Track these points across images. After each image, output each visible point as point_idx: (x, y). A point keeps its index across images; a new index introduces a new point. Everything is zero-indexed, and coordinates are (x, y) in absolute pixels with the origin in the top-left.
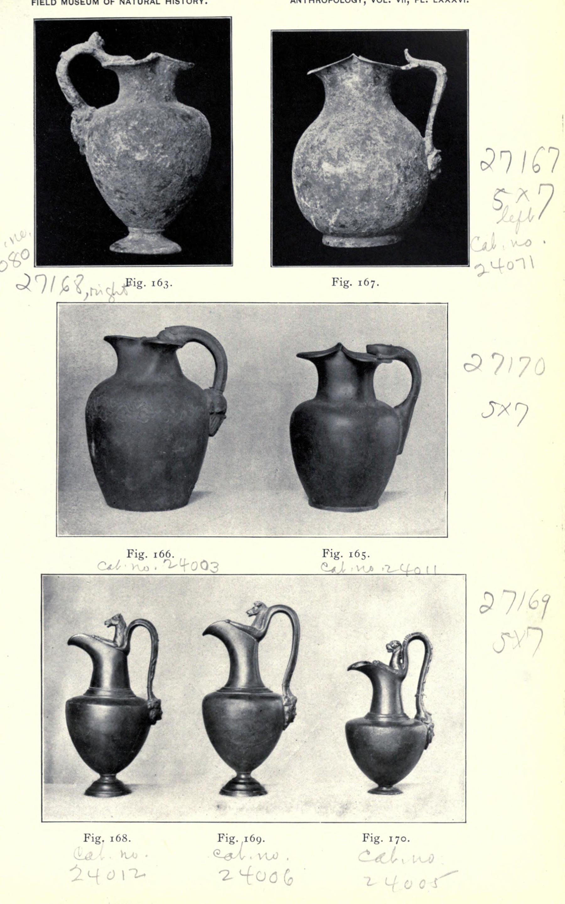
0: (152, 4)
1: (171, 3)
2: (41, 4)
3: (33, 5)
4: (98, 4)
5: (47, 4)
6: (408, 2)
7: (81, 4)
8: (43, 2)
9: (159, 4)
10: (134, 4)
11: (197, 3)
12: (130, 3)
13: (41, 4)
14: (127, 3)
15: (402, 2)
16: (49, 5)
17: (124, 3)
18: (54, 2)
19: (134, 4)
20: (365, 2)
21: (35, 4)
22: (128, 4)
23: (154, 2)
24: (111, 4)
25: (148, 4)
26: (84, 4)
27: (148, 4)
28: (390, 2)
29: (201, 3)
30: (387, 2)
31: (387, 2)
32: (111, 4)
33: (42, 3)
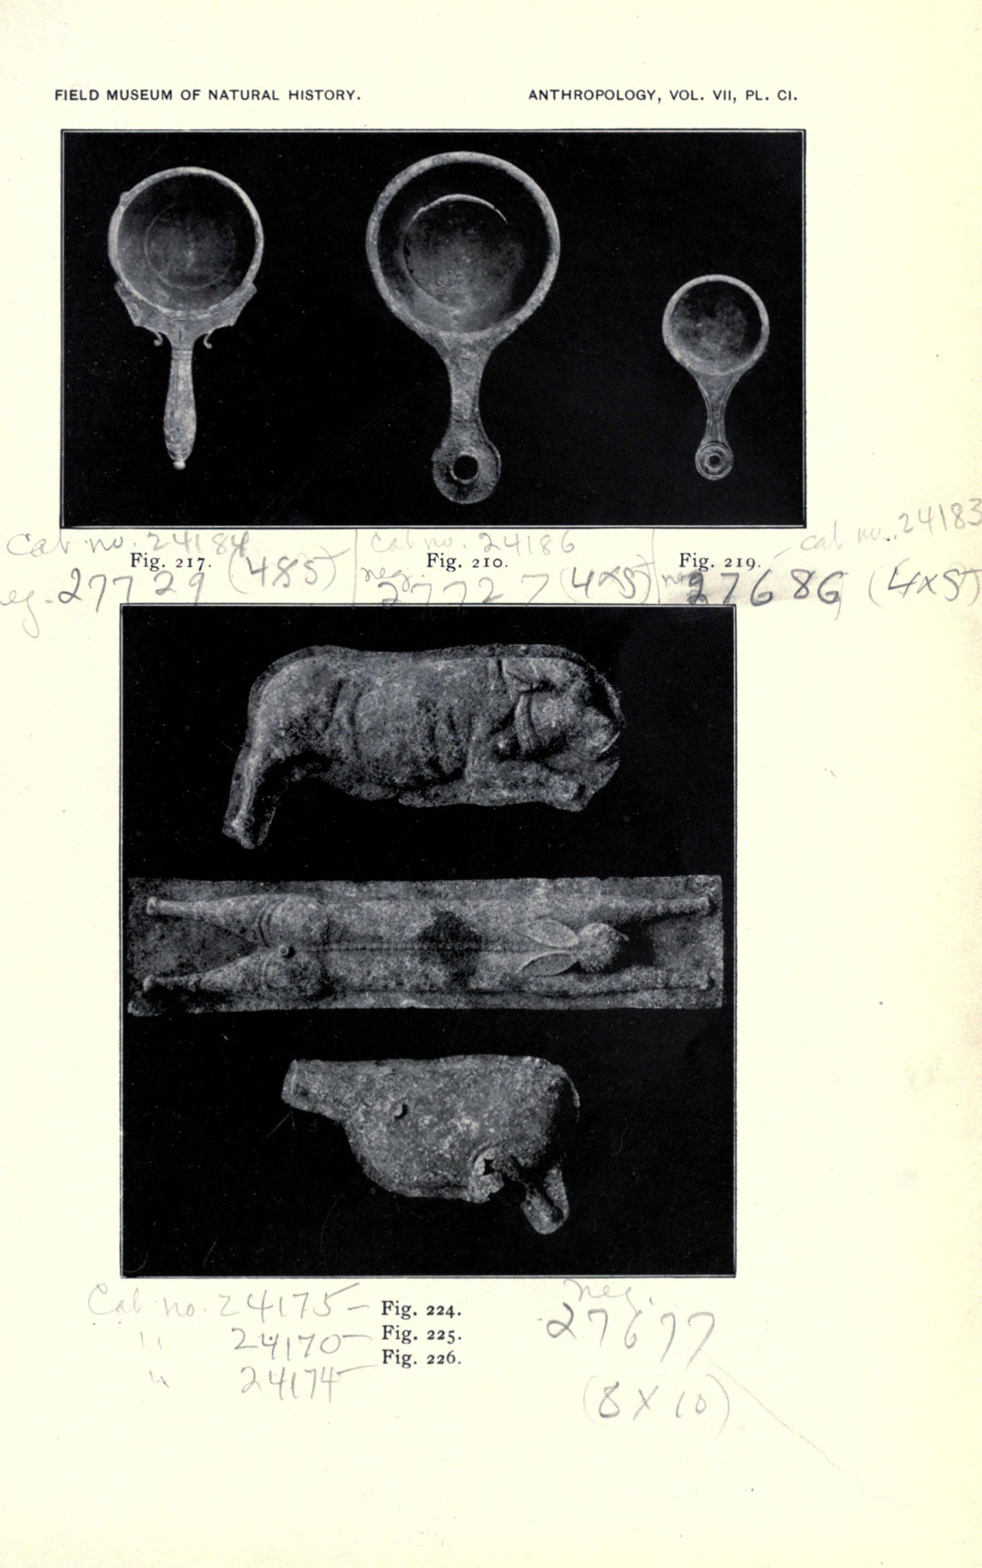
0: (266, 99)
1: (297, 98)
2: (71, 99)
3: (57, 98)
4: (171, 98)
5: (82, 99)
6: (735, 99)
7: (142, 99)
8: (75, 95)
9: (278, 99)
10: (234, 98)
11: (343, 98)
12: (226, 97)
13: (71, 99)
14: (222, 96)
15: (725, 99)
16: (85, 99)
17: (216, 97)
18: (94, 95)
19: (234, 98)
20: (659, 99)
21: (61, 98)
22: (224, 99)
23: (268, 97)
24: (194, 98)
25: (258, 99)
26: (147, 99)
27: (258, 99)
28: (702, 99)
29: (351, 98)
30: (697, 99)
31: (697, 99)
32: (194, 98)
33: (73, 97)
